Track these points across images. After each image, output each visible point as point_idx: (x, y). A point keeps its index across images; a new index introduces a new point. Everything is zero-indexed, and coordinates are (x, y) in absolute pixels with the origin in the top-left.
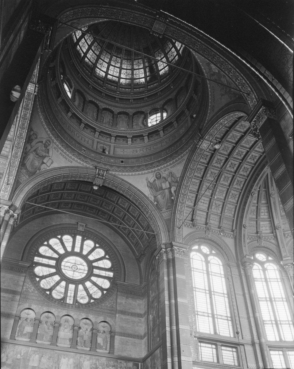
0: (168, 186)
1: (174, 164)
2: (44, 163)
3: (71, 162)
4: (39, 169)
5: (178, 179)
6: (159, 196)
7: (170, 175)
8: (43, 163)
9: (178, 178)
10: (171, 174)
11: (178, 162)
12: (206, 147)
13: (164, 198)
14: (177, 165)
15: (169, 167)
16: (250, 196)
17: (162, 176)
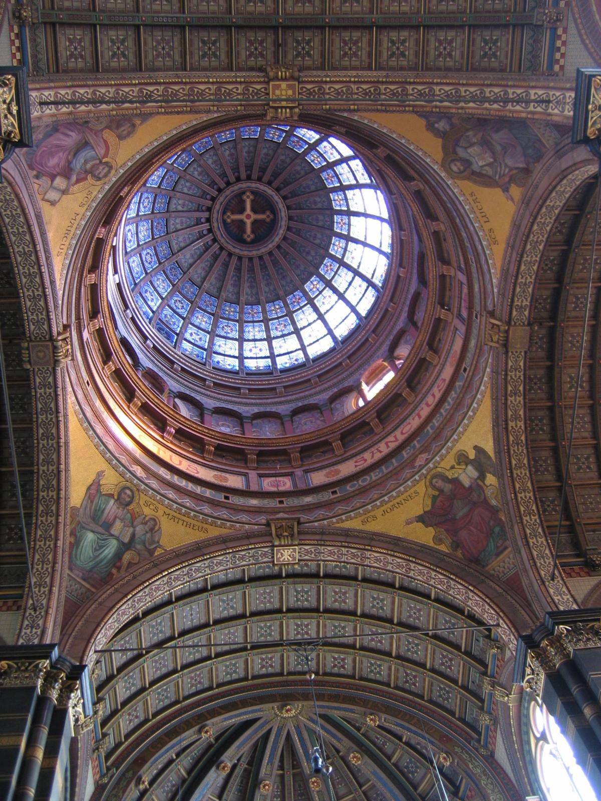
0: (126, 540)
1: (175, 514)
2: (52, 181)
3: (59, 254)
4: (37, 177)
5: (158, 552)
6: (90, 536)
7: (152, 522)
8: (53, 177)
9: (160, 547)
10: (153, 526)
11: (190, 520)
12: (281, 560)
13: (96, 550)
14: (181, 522)
15: (162, 509)
16: (197, 728)
17: (131, 507)
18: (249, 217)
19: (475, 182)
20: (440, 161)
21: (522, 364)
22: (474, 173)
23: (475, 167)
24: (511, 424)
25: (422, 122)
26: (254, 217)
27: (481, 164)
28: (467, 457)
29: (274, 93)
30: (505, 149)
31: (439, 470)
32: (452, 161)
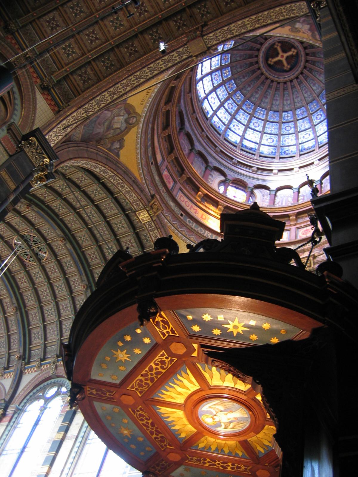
18: (282, 57)
19: (134, 109)
20: (136, 127)
21: (211, 35)
22: (129, 113)
23: (126, 116)
24: (249, 28)
25: (121, 152)
26: (281, 54)
27: (122, 117)
28: (292, 29)
29: (146, 220)
30: (104, 123)
31: (311, 38)
32: (131, 124)
